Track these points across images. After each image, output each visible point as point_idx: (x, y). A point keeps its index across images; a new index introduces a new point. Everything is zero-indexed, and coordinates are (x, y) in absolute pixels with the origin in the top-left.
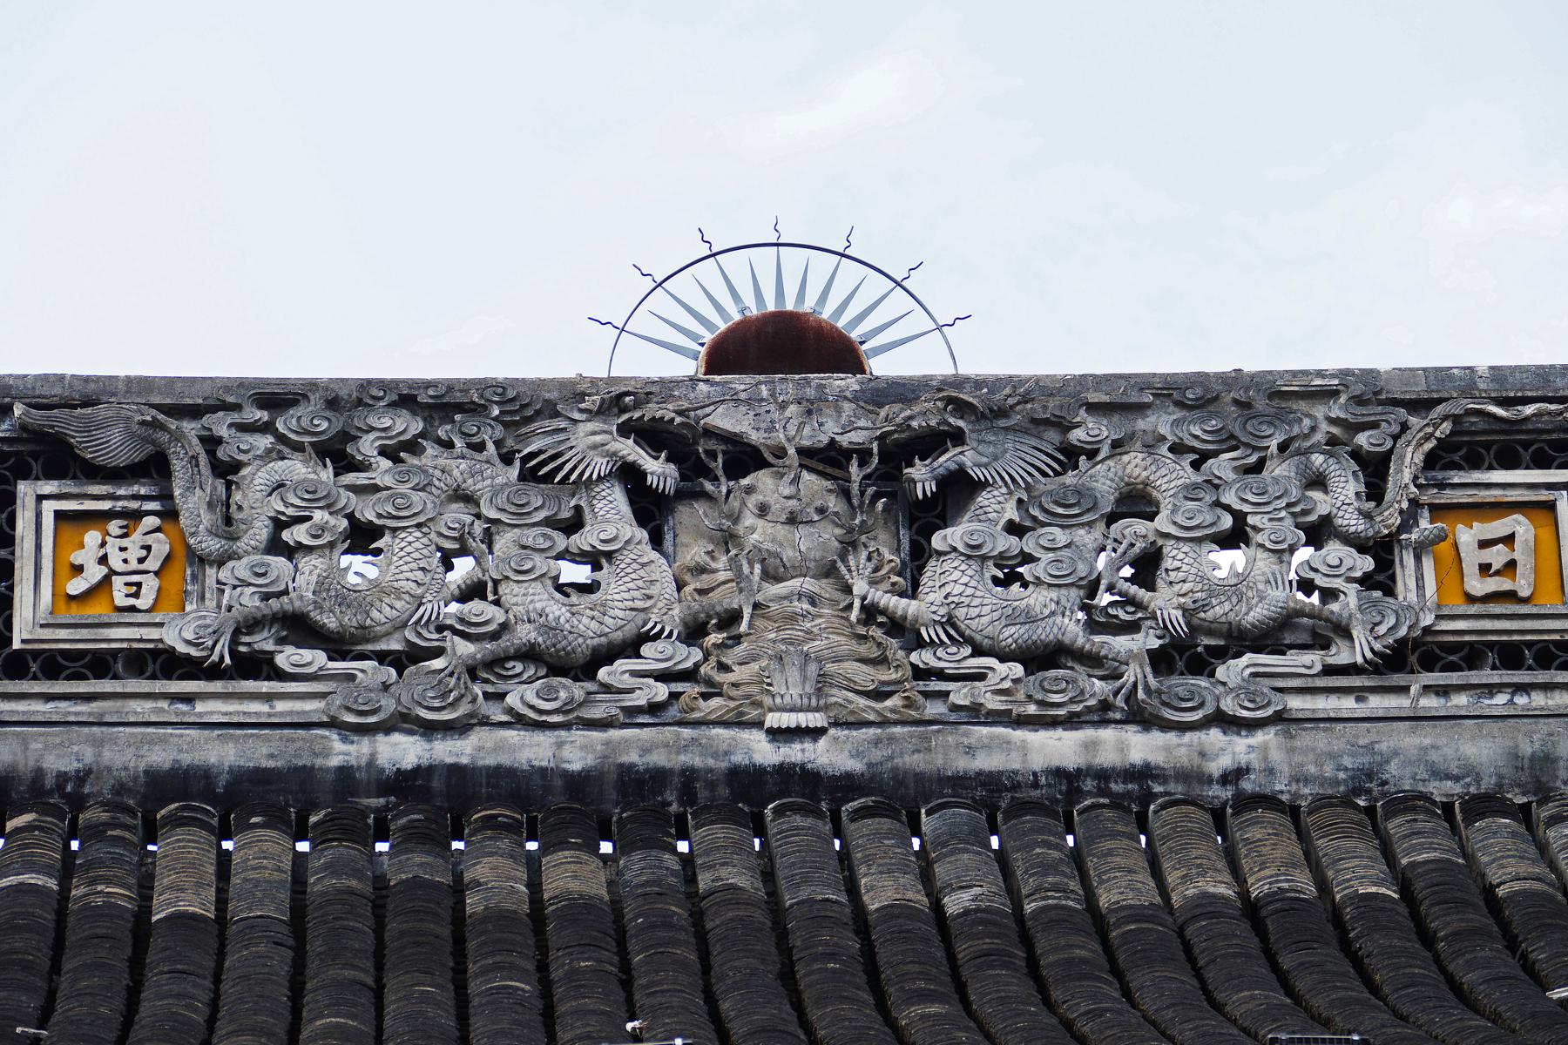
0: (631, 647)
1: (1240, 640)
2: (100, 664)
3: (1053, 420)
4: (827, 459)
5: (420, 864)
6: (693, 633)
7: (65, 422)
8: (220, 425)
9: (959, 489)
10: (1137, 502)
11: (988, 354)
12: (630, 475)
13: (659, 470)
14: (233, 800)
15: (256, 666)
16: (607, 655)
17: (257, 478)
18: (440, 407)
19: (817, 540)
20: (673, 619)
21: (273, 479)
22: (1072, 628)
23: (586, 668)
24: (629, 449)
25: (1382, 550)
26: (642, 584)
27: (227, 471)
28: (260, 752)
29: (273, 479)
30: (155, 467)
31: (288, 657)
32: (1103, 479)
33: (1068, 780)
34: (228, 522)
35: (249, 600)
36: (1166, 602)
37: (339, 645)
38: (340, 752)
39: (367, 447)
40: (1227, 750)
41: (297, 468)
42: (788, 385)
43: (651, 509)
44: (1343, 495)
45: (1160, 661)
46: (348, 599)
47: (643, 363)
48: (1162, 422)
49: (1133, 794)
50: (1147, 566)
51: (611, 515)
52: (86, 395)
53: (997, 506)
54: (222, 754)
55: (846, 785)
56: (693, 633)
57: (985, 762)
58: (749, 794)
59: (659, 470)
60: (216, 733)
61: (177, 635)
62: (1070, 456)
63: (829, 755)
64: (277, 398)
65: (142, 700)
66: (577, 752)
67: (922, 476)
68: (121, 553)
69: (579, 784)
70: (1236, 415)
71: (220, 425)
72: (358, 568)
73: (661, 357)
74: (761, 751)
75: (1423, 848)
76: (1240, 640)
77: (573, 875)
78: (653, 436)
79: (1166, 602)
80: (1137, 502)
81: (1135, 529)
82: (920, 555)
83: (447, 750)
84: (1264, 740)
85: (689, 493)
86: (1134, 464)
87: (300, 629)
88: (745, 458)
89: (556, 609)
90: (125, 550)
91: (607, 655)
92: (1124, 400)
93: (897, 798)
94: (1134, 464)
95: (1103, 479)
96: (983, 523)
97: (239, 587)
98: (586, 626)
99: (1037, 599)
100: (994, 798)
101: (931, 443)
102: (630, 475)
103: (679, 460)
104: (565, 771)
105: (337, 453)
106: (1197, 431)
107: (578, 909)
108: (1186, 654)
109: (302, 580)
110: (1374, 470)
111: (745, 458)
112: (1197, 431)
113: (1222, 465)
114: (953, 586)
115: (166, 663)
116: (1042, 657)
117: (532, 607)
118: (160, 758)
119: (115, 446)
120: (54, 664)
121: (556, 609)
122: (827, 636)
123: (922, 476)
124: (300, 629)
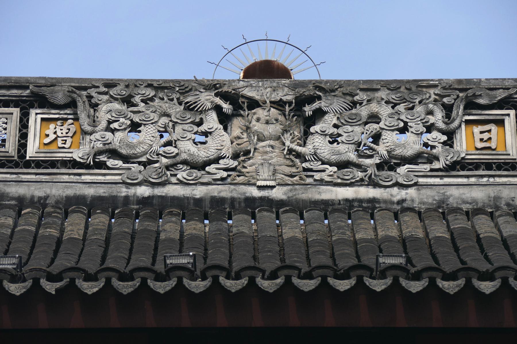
0: (216, 161)
1: (405, 160)
2: (53, 164)
3: (351, 93)
4: (279, 104)
5: (150, 225)
6: (235, 156)
7: (45, 91)
8: (93, 92)
9: (319, 114)
10: (374, 118)
11: (329, 74)
12: (218, 109)
13: (226, 107)
14: (91, 206)
15: (102, 165)
16: (209, 163)
17: (104, 108)
18: (160, 87)
19: (274, 129)
20: (228, 150)
22: (352, 156)
23: (202, 166)
24: (218, 101)
25: (450, 134)
26: (221, 142)
27: (95, 106)
28: (101, 191)
30: (72, 104)
31: (111, 163)
32: (364, 112)
33: (349, 202)
34: (94, 123)
35: (99, 145)
36: (382, 149)
37: (126, 159)
38: (124, 191)
39: (137, 99)
40: (397, 194)
41: (116, 106)
42: (268, 83)
43: (225, 120)
44: (438, 118)
45: (380, 167)
46: (130, 146)
47: (221, 75)
48: (383, 94)
49: (370, 206)
50: (377, 138)
51: (212, 121)
52: (53, 83)
53: (330, 119)
54: (90, 192)
55: (281, 203)
56: (235, 156)
57: (325, 196)
58: (251, 206)
59: (226, 107)
60: (89, 185)
61: (77, 155)
62: (354, 104)
64: (110, 84)
65: (65, 176)
66: (199, 192)
67: (308, 110)
69: (198, 202)
70: (407, 92)
71: (93, 92)
72: (133, 138)
73: (231, 73)
74: (255, 192)
75: (459, 223)
76: (405, 160)
77: (194, 227)
78: (225, 96)
79: (382, 149)
80: (374, 118)
81: (373, 127)
82: (307, 134)
83: (159, 191)
85: (236, 114)
86: (374, 107)
87: (114, 154)
88: (253, 104)
89: (193, 149)
90: (62, 130)
91: (209, 163)
92: (370, 87)
93: (297, 208)
94: (374, 107)
95: (364, 112)
96: (326, 124)
97: (97, 140)
98: (202, 154)
99: (342, 148)
100: (326, 207)
101: (311, 99)
102: (218, 109)
103: (234, 105)
104: (194, 198)
105: (128, 101)
106: (393, 97)
107: (194, 238)
108: (389, 164)
109: (117, 140)
110: (448, 109)
111: (253, 104)
112: (393, 97)
113: (401, 108)
114: (318, 144)
115: (74, 164)
116: (343, 165)
117: (187, 148)
118: (70, 192)
119: (60, 98)
120: (39, 164)
121: (193, 149)
122: (276, 158)
123: (308, 110)
124: (114, 154)
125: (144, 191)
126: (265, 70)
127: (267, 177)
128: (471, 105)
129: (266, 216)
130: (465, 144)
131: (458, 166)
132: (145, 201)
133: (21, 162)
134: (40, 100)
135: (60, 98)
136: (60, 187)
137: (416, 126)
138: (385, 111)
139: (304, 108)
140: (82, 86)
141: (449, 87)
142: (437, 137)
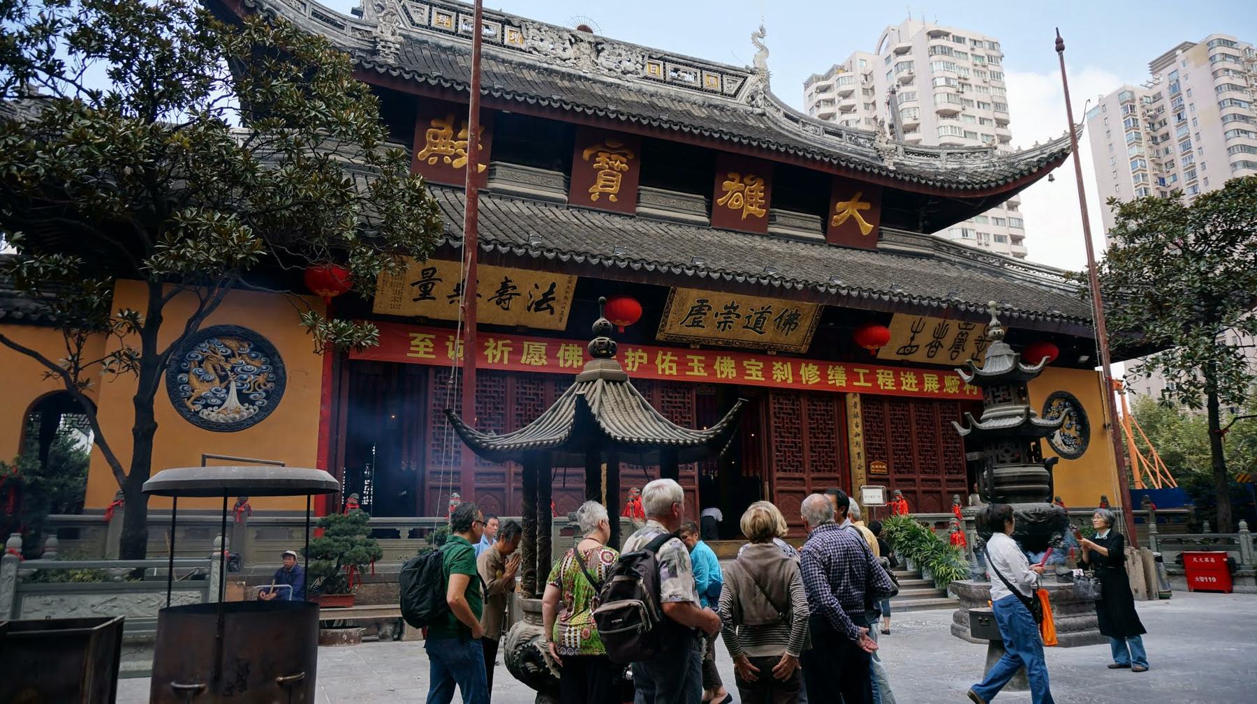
4: (590, 43)
10: (620, 55)
17: (531, 31)
18: (550, 27)
21: (532, 32)
26: (570, 52)
29: (532, 32)
30: (520, 27)
32: (617, 51)
33: (612, 84)
43: (571, 44)
44: (640, 59)
51: (567, 44)
52: (513, 17)
54: (528, 62)
63: (589, 76)
64: (533, 22)
65: (518, 53)
66: (564, 70)
68: (517, 36)
70: (631, 48)
80: (620, 55)
84: (634, 83)
87: (535, 49)
92: (619, 43)
95: (617, 51)
97: (530, 42)
98: (565, 55)
108: (624, 73)
109: (537, 44)
114: (601, 60)
117: (560, 52)
123: (600, 47)
125: (545, 65)
126: (584, 28)
127: (585, 69)
128: (650, 57)
129: (570, 80)
130: (649, 70)
131: (646, 78)
132: (546, 69)
133: (502, 45)
134: (510, 23)
135: (516, 24)
136: (517, 57)
137: (633, 61)
138: (624, 53)
139: (598, 46)
140: (524, 21)
141: (644, 49)
142: (639, 66)
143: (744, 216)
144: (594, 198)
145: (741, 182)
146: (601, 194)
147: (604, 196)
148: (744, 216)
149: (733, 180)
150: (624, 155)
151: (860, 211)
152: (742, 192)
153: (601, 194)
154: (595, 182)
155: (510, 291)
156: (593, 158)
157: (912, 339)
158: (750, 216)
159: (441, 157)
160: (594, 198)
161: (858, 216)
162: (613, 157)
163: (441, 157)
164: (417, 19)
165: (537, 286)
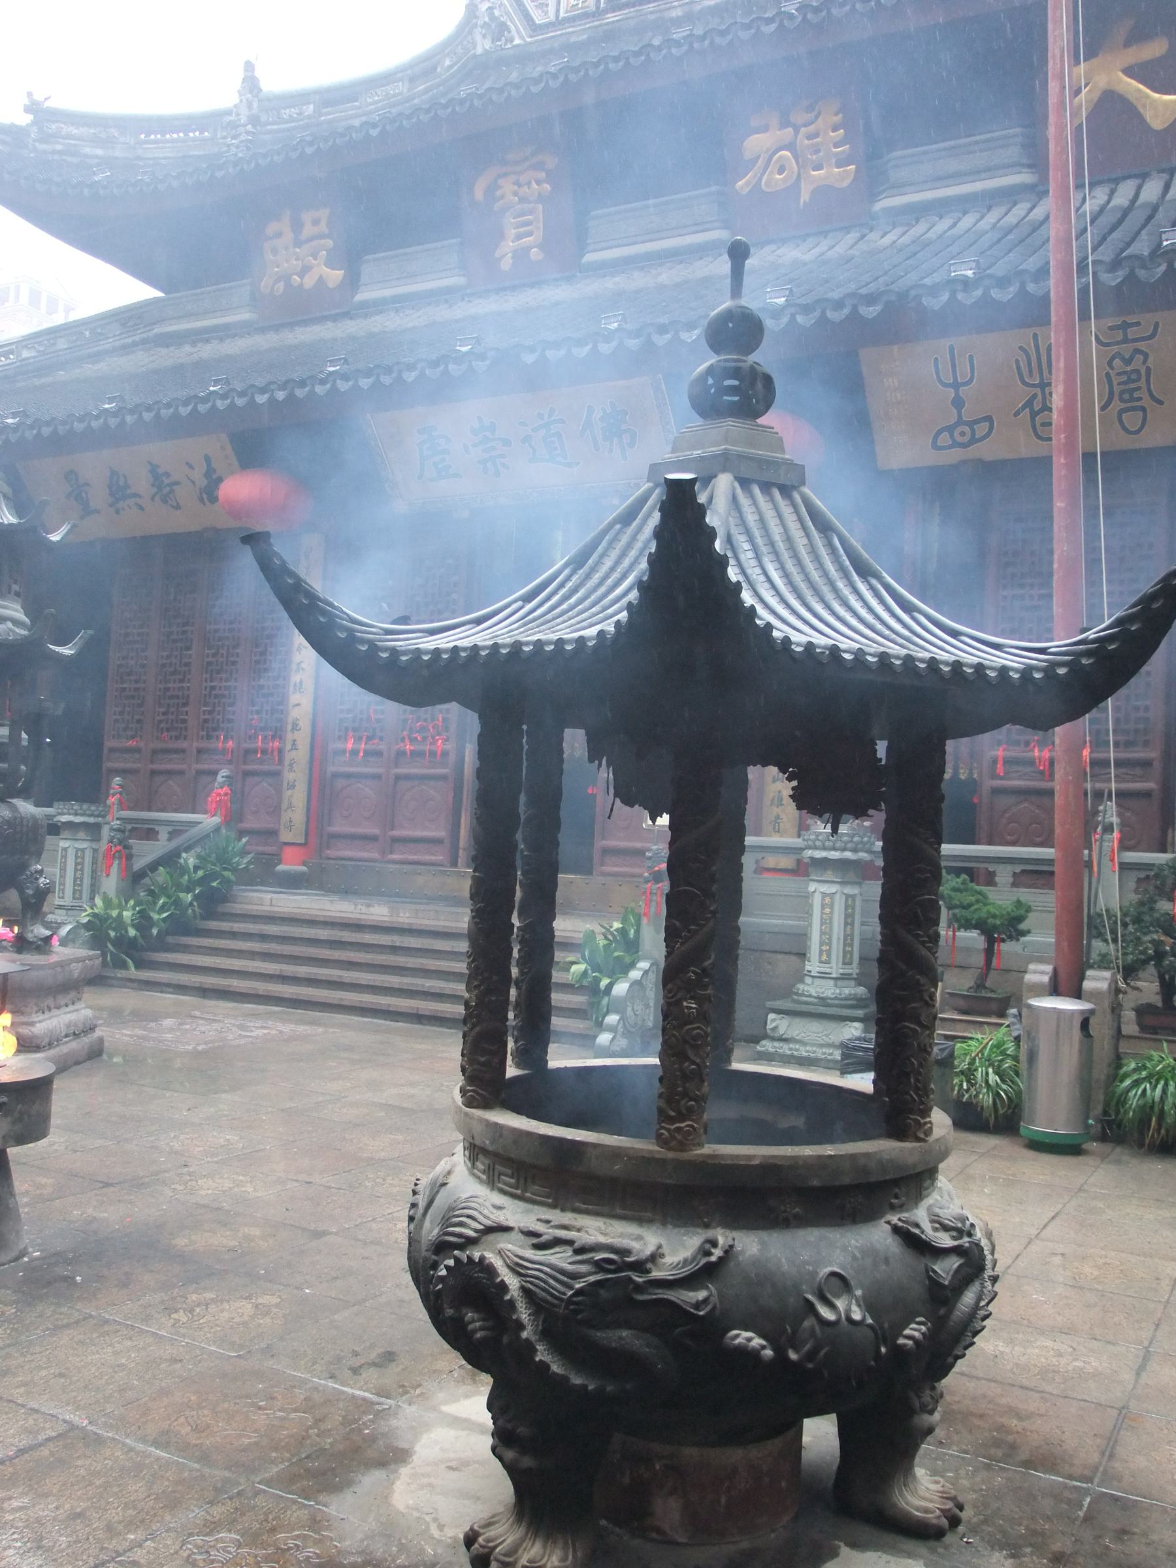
143: (805, 196)
144: (506, 264)
145: (785, 123)
146: (515, 253)
147: (521, 255)
148: (805, 196)
149: (765, 129)
150: (539, 166)
151: (1128, 72)
152: (791, 147)
153: (515, 253)
154: (502, 236)
155: (167, 481)
156: (491, 190)
157: (958, 403)
158: (822, 191)
159: (287, 278)
160: (506, 264)
161: (1132, 87)
162: (523, 178)
163: (287, 278)
164: (539, 19)
165: (191, 467)
